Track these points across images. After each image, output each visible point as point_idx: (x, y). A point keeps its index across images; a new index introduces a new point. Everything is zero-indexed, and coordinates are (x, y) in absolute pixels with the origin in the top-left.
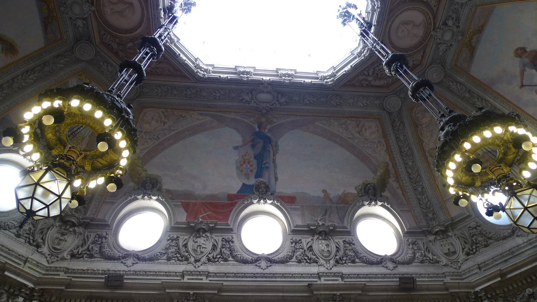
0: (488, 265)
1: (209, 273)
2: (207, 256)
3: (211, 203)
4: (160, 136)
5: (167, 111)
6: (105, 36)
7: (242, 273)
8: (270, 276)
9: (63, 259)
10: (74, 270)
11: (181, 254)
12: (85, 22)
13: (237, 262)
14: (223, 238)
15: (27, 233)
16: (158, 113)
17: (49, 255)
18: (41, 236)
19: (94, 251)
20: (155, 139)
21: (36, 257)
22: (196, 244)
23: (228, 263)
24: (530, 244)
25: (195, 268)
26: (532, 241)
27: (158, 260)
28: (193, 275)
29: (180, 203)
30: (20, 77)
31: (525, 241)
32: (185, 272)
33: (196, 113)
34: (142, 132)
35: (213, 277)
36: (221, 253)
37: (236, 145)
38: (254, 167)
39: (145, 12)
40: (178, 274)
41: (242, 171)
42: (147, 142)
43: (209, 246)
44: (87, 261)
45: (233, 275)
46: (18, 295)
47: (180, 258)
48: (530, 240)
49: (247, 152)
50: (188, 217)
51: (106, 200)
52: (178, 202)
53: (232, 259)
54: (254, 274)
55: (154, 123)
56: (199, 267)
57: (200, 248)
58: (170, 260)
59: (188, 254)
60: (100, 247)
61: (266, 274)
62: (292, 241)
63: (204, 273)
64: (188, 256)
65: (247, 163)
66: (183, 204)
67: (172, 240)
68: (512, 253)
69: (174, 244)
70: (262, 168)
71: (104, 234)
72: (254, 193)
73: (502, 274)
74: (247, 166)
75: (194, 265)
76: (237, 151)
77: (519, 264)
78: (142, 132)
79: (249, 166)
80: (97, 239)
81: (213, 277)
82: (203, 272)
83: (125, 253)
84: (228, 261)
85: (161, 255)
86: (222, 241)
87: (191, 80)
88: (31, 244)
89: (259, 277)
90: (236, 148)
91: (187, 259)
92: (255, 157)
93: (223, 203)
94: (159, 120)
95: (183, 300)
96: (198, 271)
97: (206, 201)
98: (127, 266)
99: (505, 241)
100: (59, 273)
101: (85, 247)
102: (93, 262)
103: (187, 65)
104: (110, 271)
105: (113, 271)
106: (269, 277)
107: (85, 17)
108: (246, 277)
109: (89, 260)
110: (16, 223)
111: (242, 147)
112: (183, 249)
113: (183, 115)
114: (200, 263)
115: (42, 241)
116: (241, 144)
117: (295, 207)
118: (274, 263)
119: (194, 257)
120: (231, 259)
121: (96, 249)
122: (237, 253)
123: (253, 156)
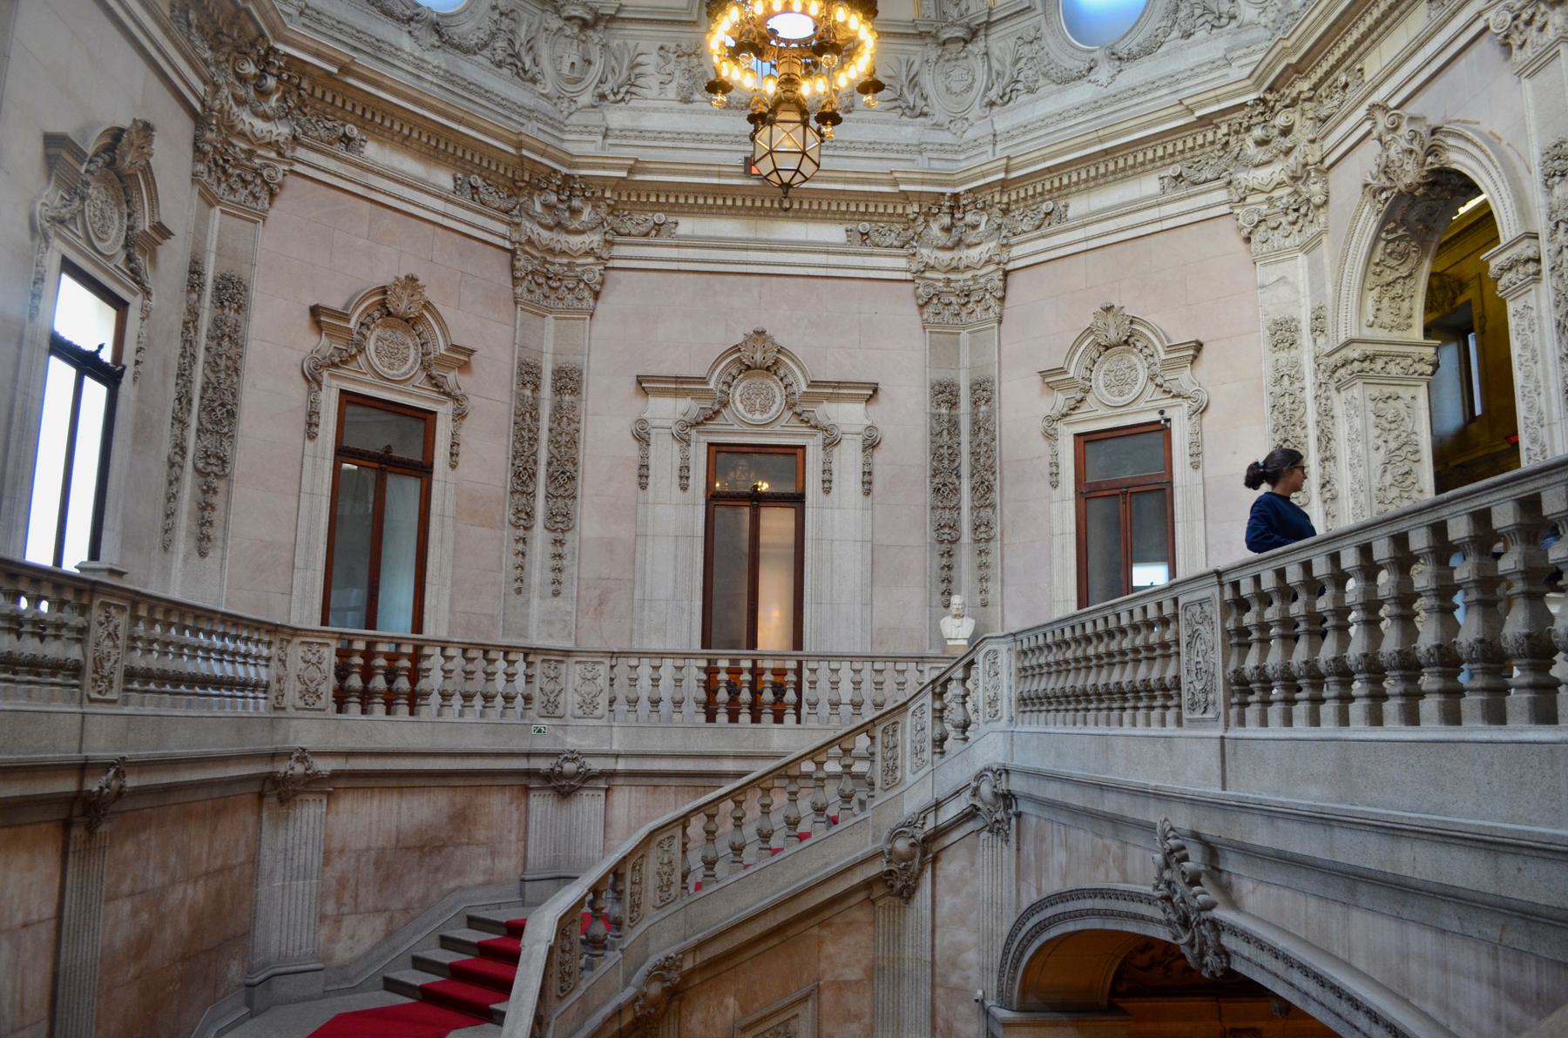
0: (319, 22)
24: (418, 67)
26: (425, 65)
31: (417, 54)
48: (423, 60)
68: (378, 49)
73: (345, 69)
77: (386, 81)
99: (383, 17)
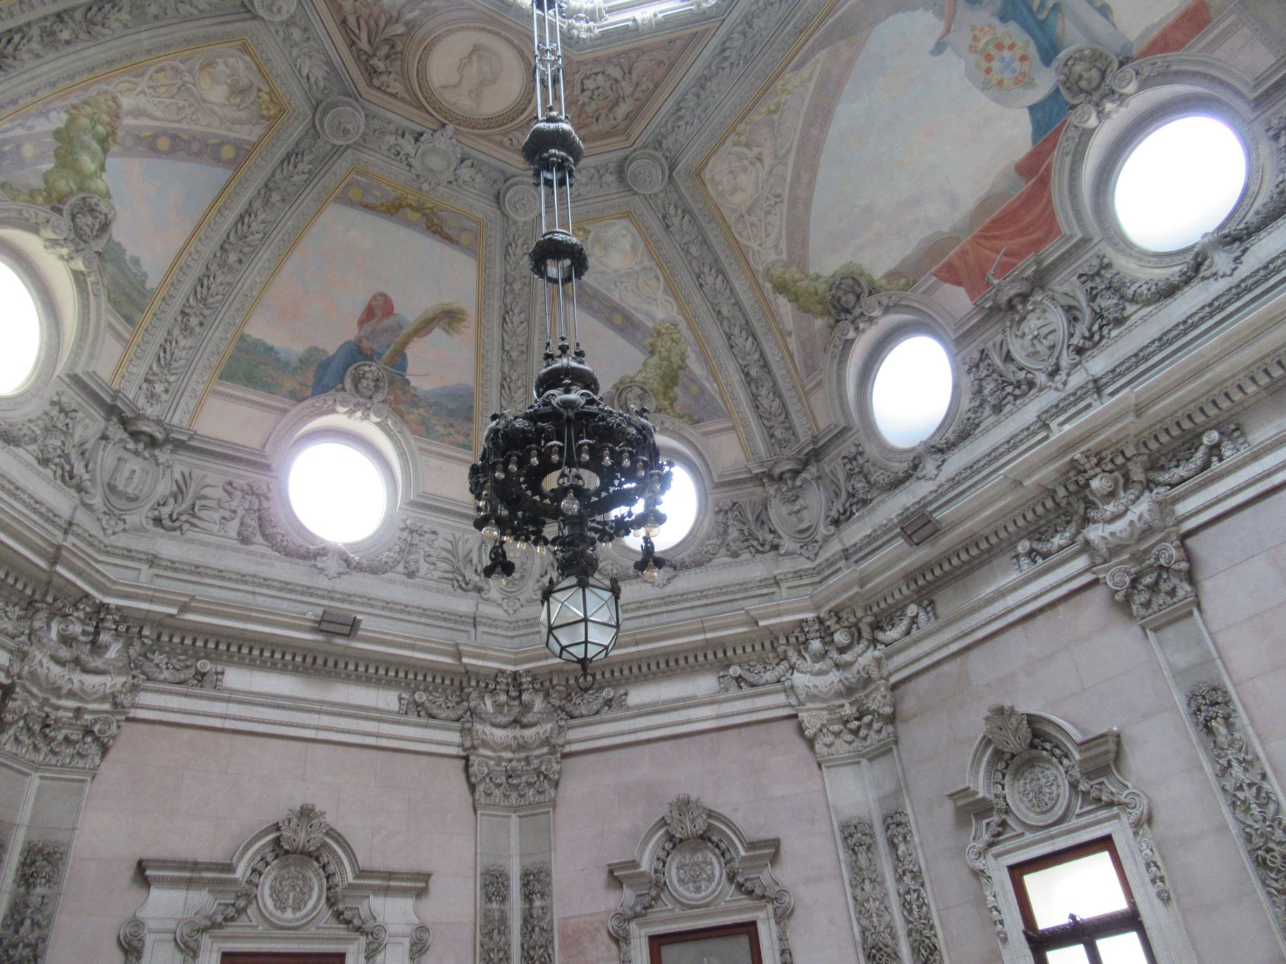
1: (1095, 381)
2: (1069, 346)
3: (994, 221)
4: (778, 191)
5: (739, 134)
6: (515, 142)
7: (1177, 325)
8: (1257, 278)
9: (827, 539)
10: (855, 545)
11: (1011, 384)
12: (468, 162)
13: (1149, 305)
14: (1081, 276)
15: (743, 542)
16: (730, 153)
17: (802, 547)
18: (766, 528)
19: (861, 491)
20: (776, 203)
21: (786, 566)
23: (1128, 323)
25: (1058, 393)
27: (978, 425)
28: (1064, 410)
29: (934, 279)
30: (506, 338)
32: (1044, 417)
33: (788, 76)
34: (742, 216)
35: (1113, 381)
36: (1098, 315)
37: (931, 42)
38: (1020, 44)
39: (503, 33)
40: (1032, 428)
41: (1000, 83)
42: (769, 224)
43: (1057, 319)
44: (862, 516)
45: (1157, 344)
46: (807, 640)
47: (1017, 392)
49: (973, 29)
50: (972, 293)
51: (807, 389)
52: (927, 279)
53: (1134, 308)
54: (1210, 305)
55: (742, 178)
56: (1065, 384)
57: (1041, 342)
58: (1001, 411)
59: (1024, 372)
60: (865, 477)
61: (1243, 280)
62: (1271, 133)
63: (1084, 390)
64: (1029, 376)
65: (993, 52)
66: (941, 274)
67: (977, 366)
69: (985, 373)
70: (1041, 24)
71: (853, 450)
72: (1073, 107)
74: (1002, 60)
75: (1053, 385)
76: (948, 50)
78: (742, 216)
79: (1006, 54)
80: (849, 466)
81: (1114, 382)
82: (1082, 387)
83: (912, 455)
84: (1125, 319)
85: (975, 412)
87: (706, 31)
88: (763, 552)
89: (1229, 302)
90: (939, 48)
91: (1031, 384)
92: (1003, 18)
93: (1021, 195)
94: (746, 162)
95: (1074, 478)
96: (1069, 395)
97: (981, 226)
98: (930, 479)
100: (838, 566)
101: (844, 495)
102: (873, 509)
103: (667, 19)
104: (908, 508)
105: (914, 504)
106: (1257, 284)
107: (459, 156)
108: (1194, 326)
109: (865, 510)
110: (715, 541)
111: (948, 31)
112: (1009, 371)
113: (772, 107)
114: (1063, 374)
115: (772, 536)
116: (940, 26)
117: (1222, 27)
118: (1249, 235)
120: (1130, 309)
121: (860, 485)
122: (1133, 288)
123: (996, 22)
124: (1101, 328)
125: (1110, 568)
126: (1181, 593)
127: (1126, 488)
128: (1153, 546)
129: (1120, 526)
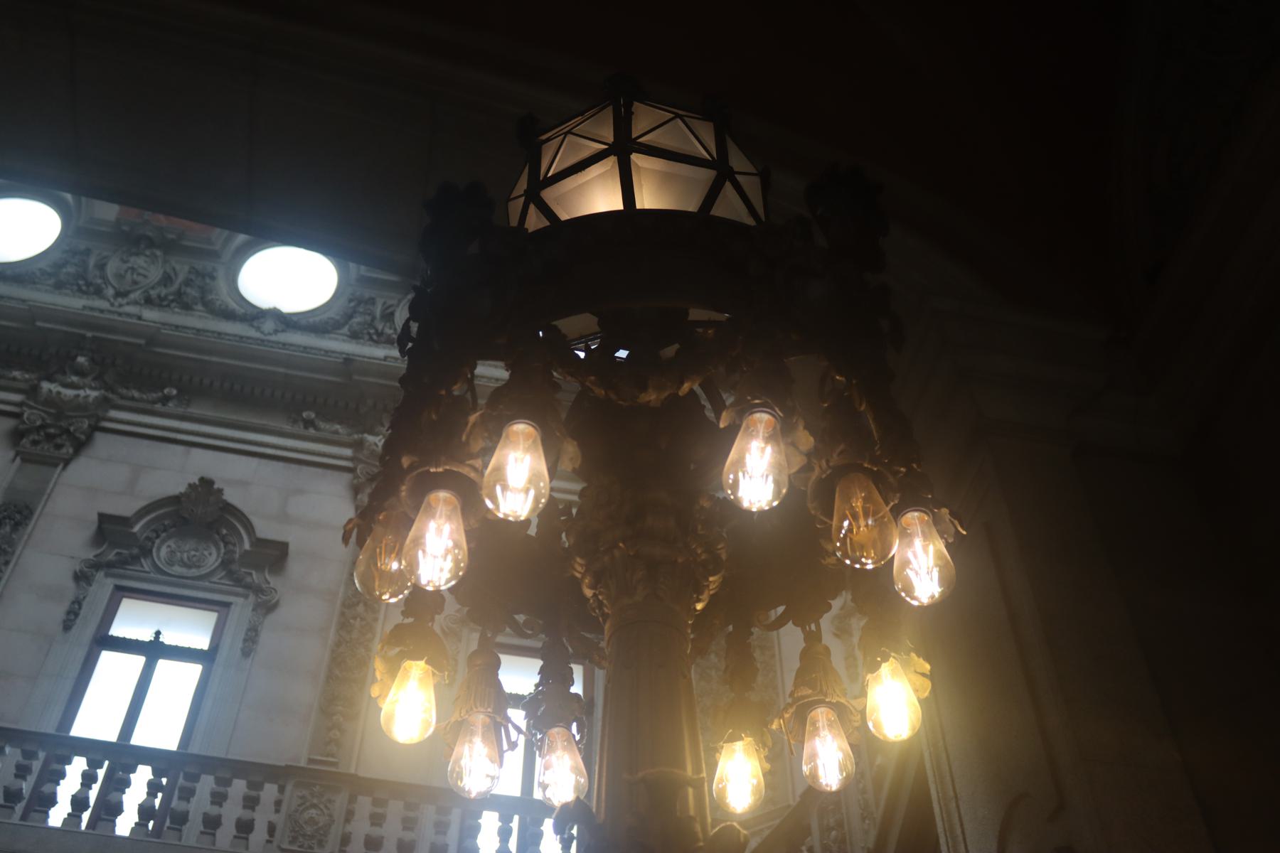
22: (125, 266)
36: (179, 294)
43: (155, 274)
56: (121, 305)
57: (133, 274)
86: (190, 272)
114: (125, 301)
119: (113, 287)
120: (200, 307)
124: (172, 301)
125: (35, 408)
126: (64, 450)
127: (95, 379)
128: (76, 417)
129: (70, 393)
